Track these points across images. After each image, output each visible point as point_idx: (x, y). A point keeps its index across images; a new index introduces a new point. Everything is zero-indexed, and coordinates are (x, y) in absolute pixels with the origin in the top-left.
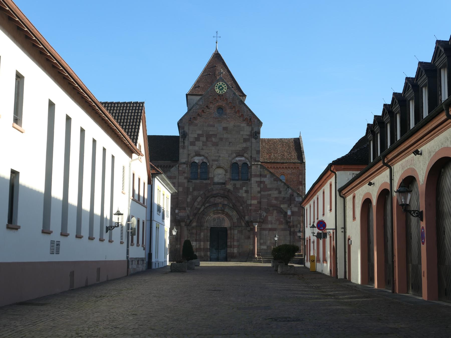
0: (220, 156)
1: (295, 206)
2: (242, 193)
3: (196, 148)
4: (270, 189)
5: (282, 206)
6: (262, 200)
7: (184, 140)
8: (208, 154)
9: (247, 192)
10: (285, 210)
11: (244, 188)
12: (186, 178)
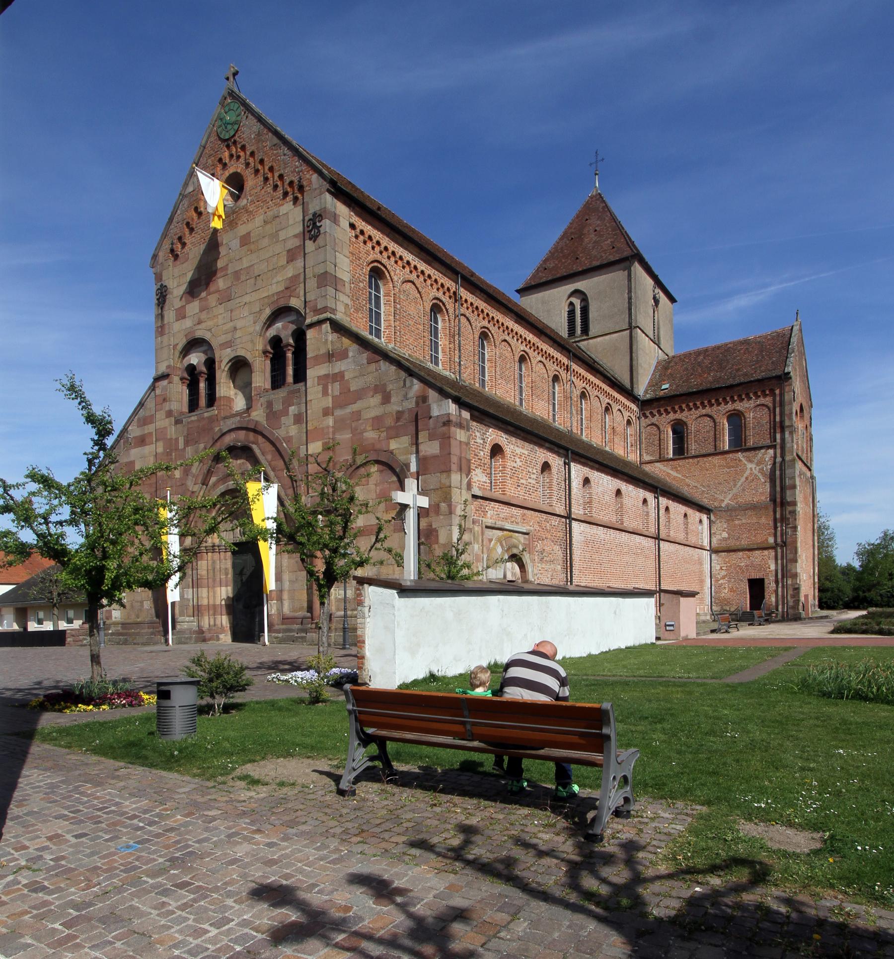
0: (235, 329)
1: (431, 438)
2: (288, 429)
3: (188, 323)
4: (359, 395)
5: (393, 445)
6: (338, 436)
7: (162, 309)
8: (210, 330)
9: (299, 419)
10: (402, 458)
11: (292, 409)
12: (169, 414)
